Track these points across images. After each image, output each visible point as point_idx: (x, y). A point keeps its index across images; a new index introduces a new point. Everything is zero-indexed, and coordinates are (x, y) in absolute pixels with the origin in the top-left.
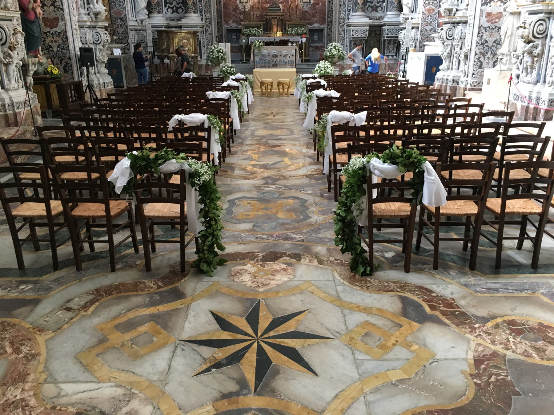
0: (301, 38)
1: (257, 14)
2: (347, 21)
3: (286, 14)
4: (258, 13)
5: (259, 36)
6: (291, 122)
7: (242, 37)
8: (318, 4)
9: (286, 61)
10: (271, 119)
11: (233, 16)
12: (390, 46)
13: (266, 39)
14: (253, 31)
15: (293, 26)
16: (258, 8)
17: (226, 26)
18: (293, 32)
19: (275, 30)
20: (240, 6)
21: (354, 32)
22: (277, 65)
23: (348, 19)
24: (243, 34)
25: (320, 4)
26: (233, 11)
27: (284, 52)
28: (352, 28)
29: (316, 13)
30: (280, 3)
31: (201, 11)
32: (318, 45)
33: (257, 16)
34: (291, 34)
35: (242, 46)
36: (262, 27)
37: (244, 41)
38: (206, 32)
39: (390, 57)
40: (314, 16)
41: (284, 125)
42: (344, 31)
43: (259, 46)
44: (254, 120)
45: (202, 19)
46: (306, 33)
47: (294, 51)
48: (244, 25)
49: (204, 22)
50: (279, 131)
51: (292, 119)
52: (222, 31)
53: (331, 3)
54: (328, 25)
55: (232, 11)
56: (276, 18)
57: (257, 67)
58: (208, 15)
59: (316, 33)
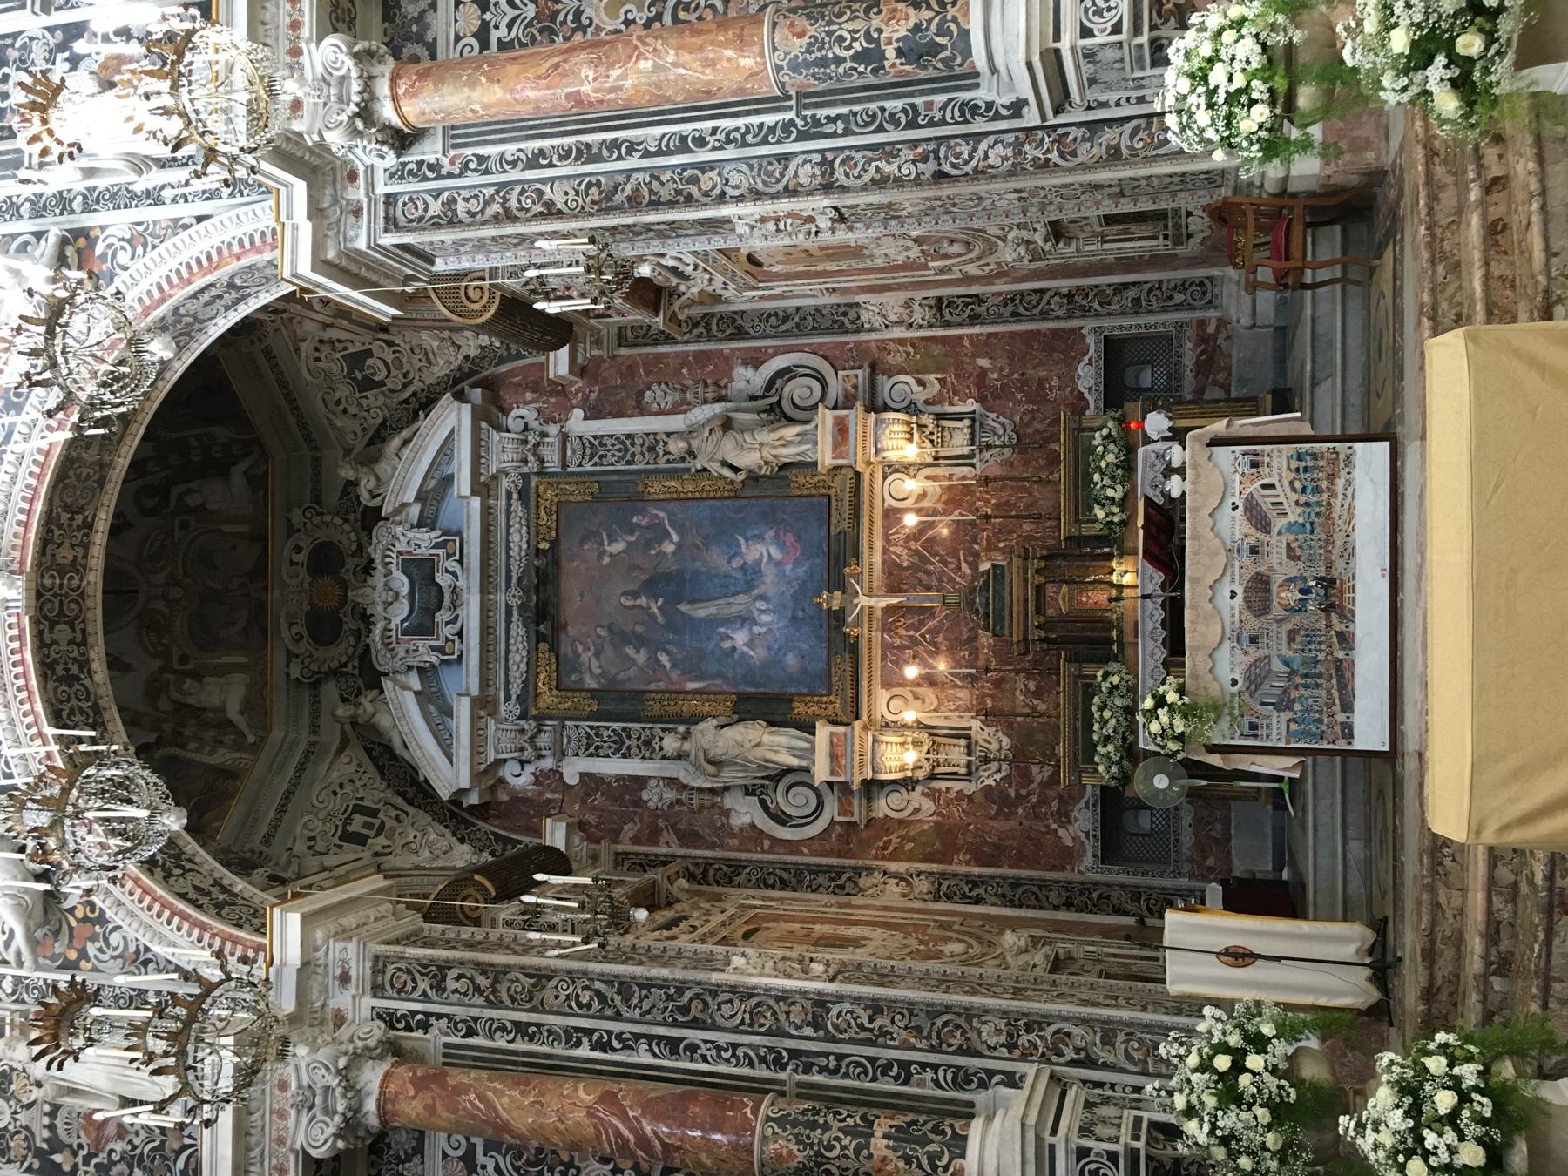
0: (1148, 440)
1: (1027, 692)
2: (1031, 118)
3: (1029, 538)
4: (1020, 690)
5: (1133, 690)
7: (1138, 788)
8: (984, 372)
9: (1294, 515)
11: (1037, 816)
13: (1149, 651)
14: (1106, 722)
15: (1084, 497)
16: (997, 683)
17: (1088, 860)
18: (1116, 493)
19: (1100, 597)
20: (989, 777)
21: (1095, 23)
22: (1328, 583)
23: (1017, 108)
24: (1125, 779)
25: (984, 362)
26: (1008, 818)
27: (1234, 525)
28: (1065, 45)
29: (1024, 381)
30: (974, 566)
31: (962, 1079)
32: (1189, 361)
33: (1038, 694)
34: (1125, 503)
35: (1193, 794)
36: (1088, 668)
37: (1161, 782)
38: (1090, 1063)
40: (1038, 394)
42: (1093, 127)
43: (1187, 712)
45: (1012, 1081)
46: (1122, 421)
47: (1222, 452)
48: (1077, 770)
49: (1029, 1069)
52: (1109, 885)
53: (979, 309)
54: (1085, 312)
55: (1012, 824)
56: (1039, 589)
57: (1348, 731)
58: (990, 1034)
59: (1130, 371)
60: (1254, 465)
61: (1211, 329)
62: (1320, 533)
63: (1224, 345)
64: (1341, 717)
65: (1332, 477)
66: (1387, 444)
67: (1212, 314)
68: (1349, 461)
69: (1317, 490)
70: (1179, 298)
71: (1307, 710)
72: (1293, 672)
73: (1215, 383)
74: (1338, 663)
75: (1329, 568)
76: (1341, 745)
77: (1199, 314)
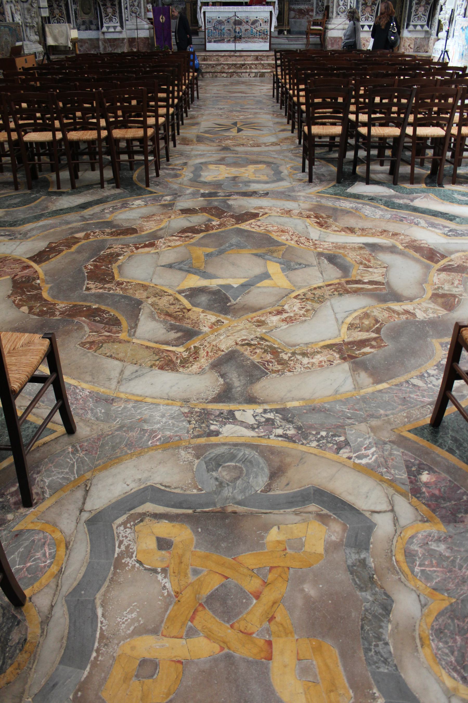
6: (273, 144)
10: (234, 138)
12: (420, 9)
22: (240, 38)
32: (302, 7)
39: (419, 28)
41: (259, 153)
44: (200, 139)
47: (268, 15)
50: (251, 168)
51: (273, 139)
57: (210, 42)
60: (266, 22)
61: (311, 13)
62: (250, 36)
63: (306, 17)
64: (213, 40)
65: (262, 38)
66: (268, 49)
67: (314, 13)
68: (265, 42)
69: (260, 35)
70: (320, 4)
71: (214, 33)
72: (221, 30)
73: (296, 14)
74: (224, 40)
75: (244, 38)
76: (207, 41)
77: (315, 10)
